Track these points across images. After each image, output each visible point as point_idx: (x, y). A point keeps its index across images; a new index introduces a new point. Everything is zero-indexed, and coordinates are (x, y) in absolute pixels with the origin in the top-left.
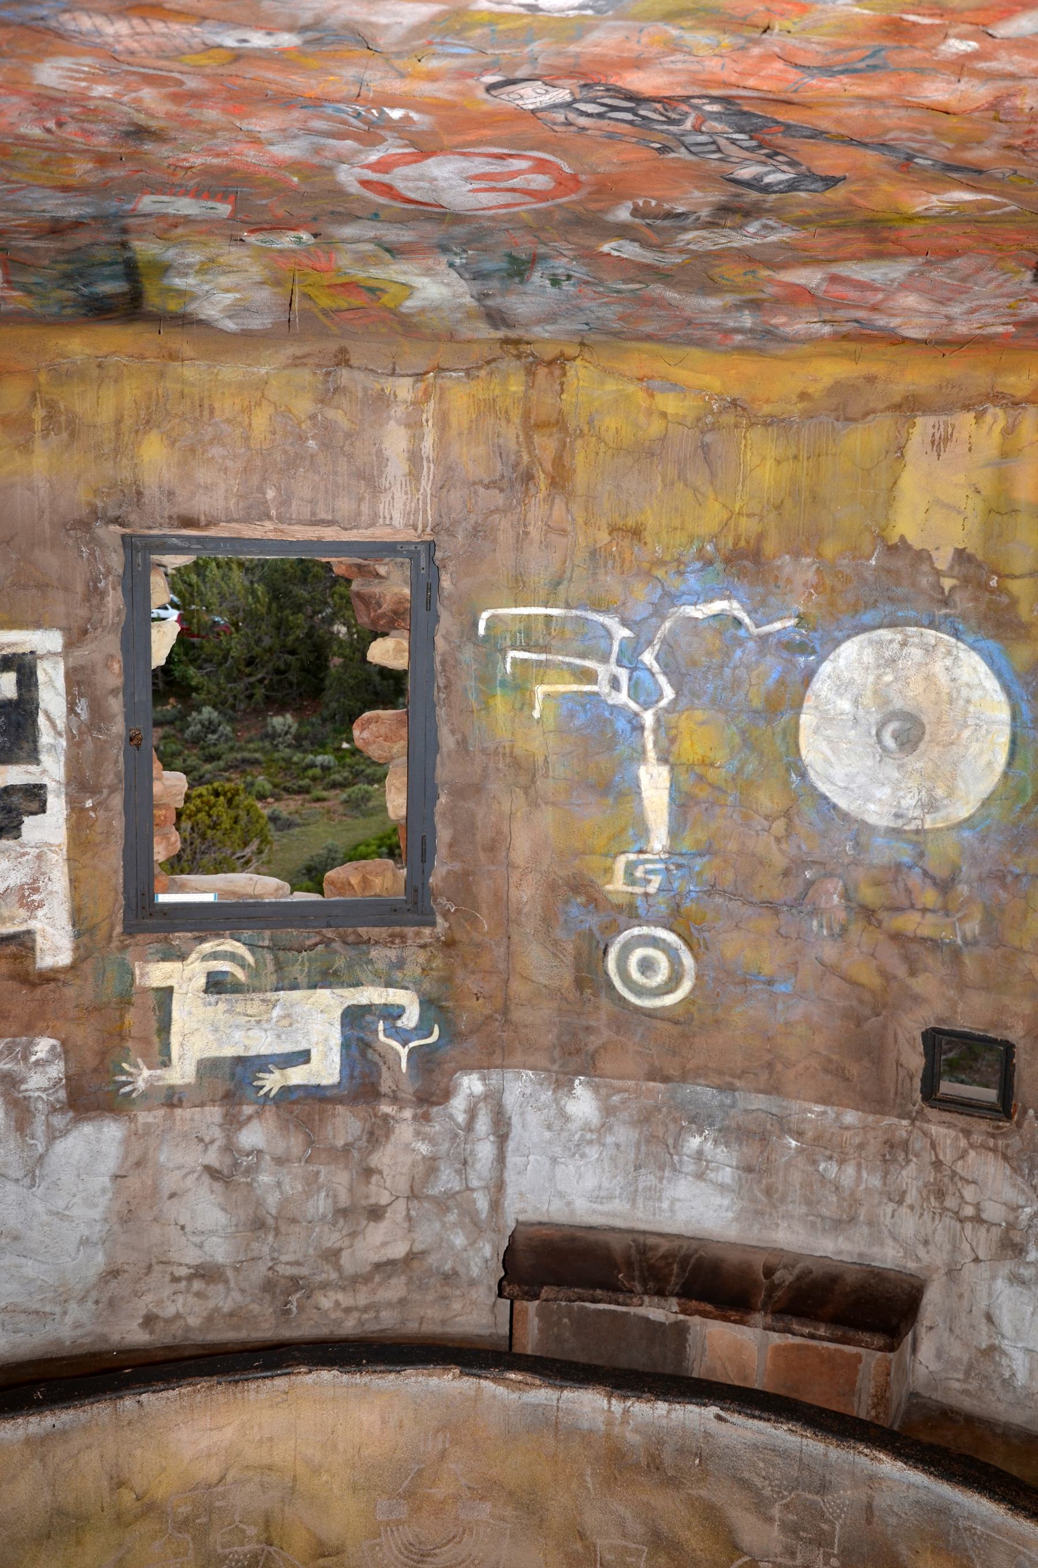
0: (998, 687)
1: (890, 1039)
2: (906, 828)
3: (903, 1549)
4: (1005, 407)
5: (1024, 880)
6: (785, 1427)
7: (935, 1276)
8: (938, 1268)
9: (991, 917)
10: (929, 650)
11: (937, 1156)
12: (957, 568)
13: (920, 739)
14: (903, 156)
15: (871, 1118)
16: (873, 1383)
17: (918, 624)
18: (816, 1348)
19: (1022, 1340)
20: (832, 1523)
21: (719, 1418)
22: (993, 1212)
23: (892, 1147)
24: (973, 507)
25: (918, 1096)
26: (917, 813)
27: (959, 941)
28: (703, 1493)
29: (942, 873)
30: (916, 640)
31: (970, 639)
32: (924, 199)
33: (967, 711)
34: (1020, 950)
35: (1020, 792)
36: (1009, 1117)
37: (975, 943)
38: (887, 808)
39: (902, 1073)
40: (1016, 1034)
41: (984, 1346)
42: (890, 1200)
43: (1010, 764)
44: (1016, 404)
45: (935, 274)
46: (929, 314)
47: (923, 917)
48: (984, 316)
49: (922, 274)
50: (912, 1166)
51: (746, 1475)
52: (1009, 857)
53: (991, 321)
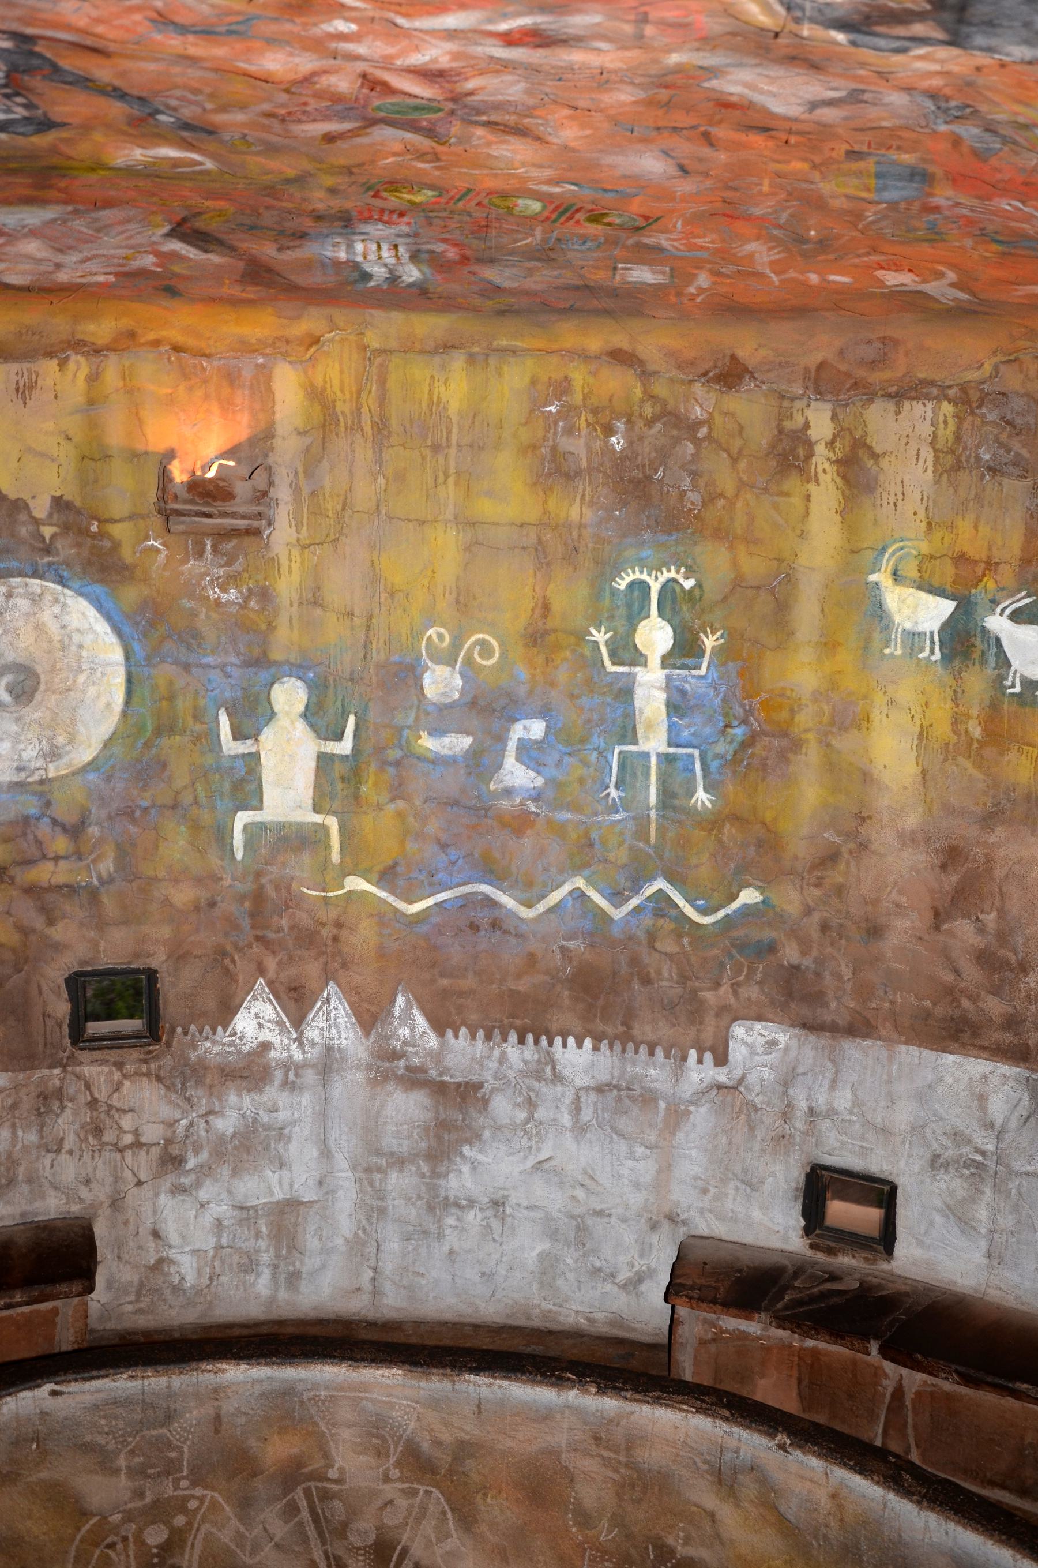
0: (109, 630)
1: (34, 992)
2: (30, 780)
3: (253, 1442)
4: (86, 354)
5: (153, 811)
6: (125, 1376)
7: (100, 1212)
8: (102, 1203)
9: (123, 854)
10: (35, 599)
11: (92, 1095)
12: (55, 516)
13: (35, 690)
14: (148, 111)
15: (21, 1076)
16: (72, 1331)
17: (21, 574)
18: (11, 1317)
19: (188, 1244)
20: (180, 1449)
21: (54, 1393)
22: (152, 1133)
23: (45, 1098)
24: (66, 454)
25: (67, 1041)
26: (40, 763)
27: (95, 882)
28: (44, 1475)
29: (70, 818)
30: (21, 590)
31: (77, 584)
32: (126, 152)
33: (81, 656)
34: (156, 879)
35: (141, 728)
36: (157, 1040)
37: (111, 880)
38: (8, 763)
39: (50, 1023)
40: (158, 960)
41: (152, 1262)
42: (48, 1151)
43: (128, 702)
44: (97, 352)
45: (79, 225)
46: (39, 261)
47: (56, 865)
48: (92, 266)
49: (65, 222)
50: (68, 1112)
51: (88, 1438)
52: (135, 792)
53: (94, 270)
